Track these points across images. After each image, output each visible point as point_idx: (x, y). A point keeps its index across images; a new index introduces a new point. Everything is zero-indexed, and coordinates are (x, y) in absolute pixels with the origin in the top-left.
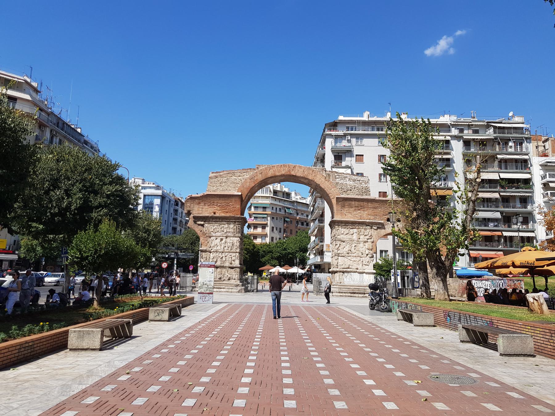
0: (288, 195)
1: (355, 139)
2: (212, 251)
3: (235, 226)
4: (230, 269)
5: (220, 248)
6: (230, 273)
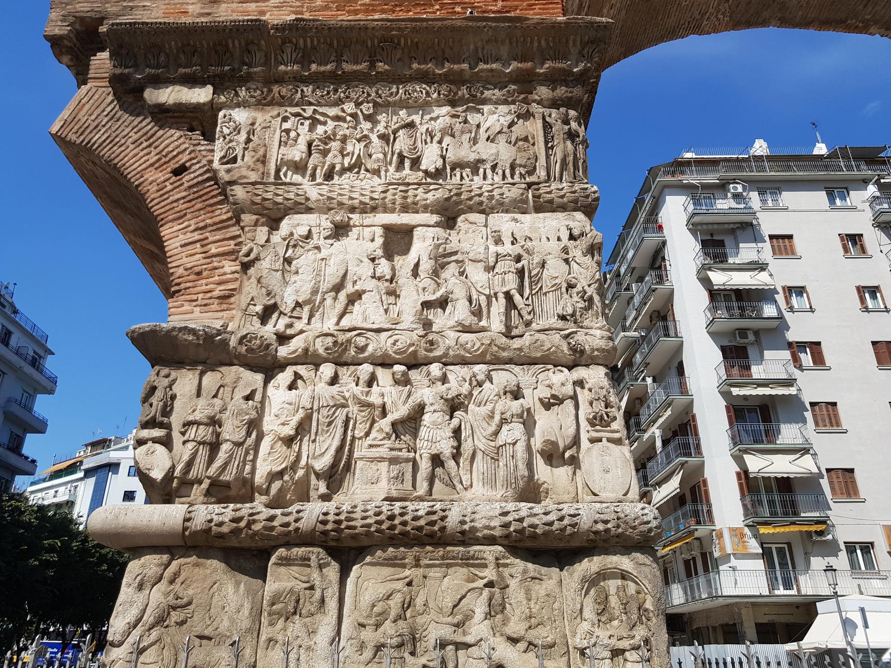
1: (757, 193)
3: (527, 116)
5: (378, 319)
6: (532, 621)
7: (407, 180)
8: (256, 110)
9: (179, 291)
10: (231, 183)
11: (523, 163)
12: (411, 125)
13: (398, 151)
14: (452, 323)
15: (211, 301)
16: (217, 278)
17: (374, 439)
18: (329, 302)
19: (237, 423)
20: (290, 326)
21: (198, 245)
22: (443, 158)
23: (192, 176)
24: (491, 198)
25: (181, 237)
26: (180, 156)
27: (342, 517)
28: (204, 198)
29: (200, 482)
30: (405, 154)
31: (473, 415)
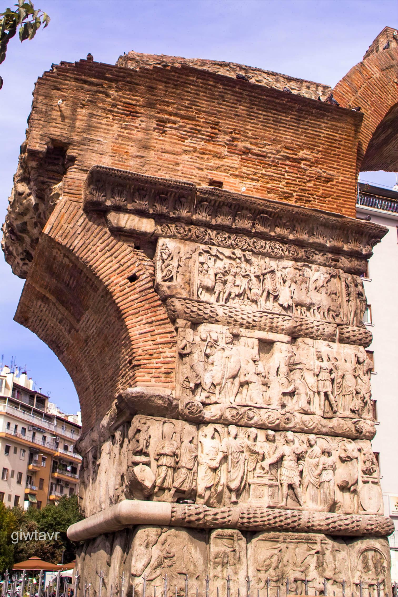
0: (42, 400)
2: (209, 413)
4: (330, 543)
7: (273, 312)
8: (180, 242)
9: (140, 365)
10: (171, 296)
11: (334, 310)
12: (273, 272)
13: (267, 290)
14: (297, 408)
15: (160, 375)
16: (162, 359)
17: (260, 473)
18: (229, 384)
19: (188, 457)
20: (207, 397)
21: (149, 334)
22: (292, 298)
23: (142, 283)
24: (318, 330)
25: (138, 327)
26: (132, 266)
27: (251, 516)
28: (150, 301)
29: (170, 490)
30: (271, 292)
31: (307, 463)
